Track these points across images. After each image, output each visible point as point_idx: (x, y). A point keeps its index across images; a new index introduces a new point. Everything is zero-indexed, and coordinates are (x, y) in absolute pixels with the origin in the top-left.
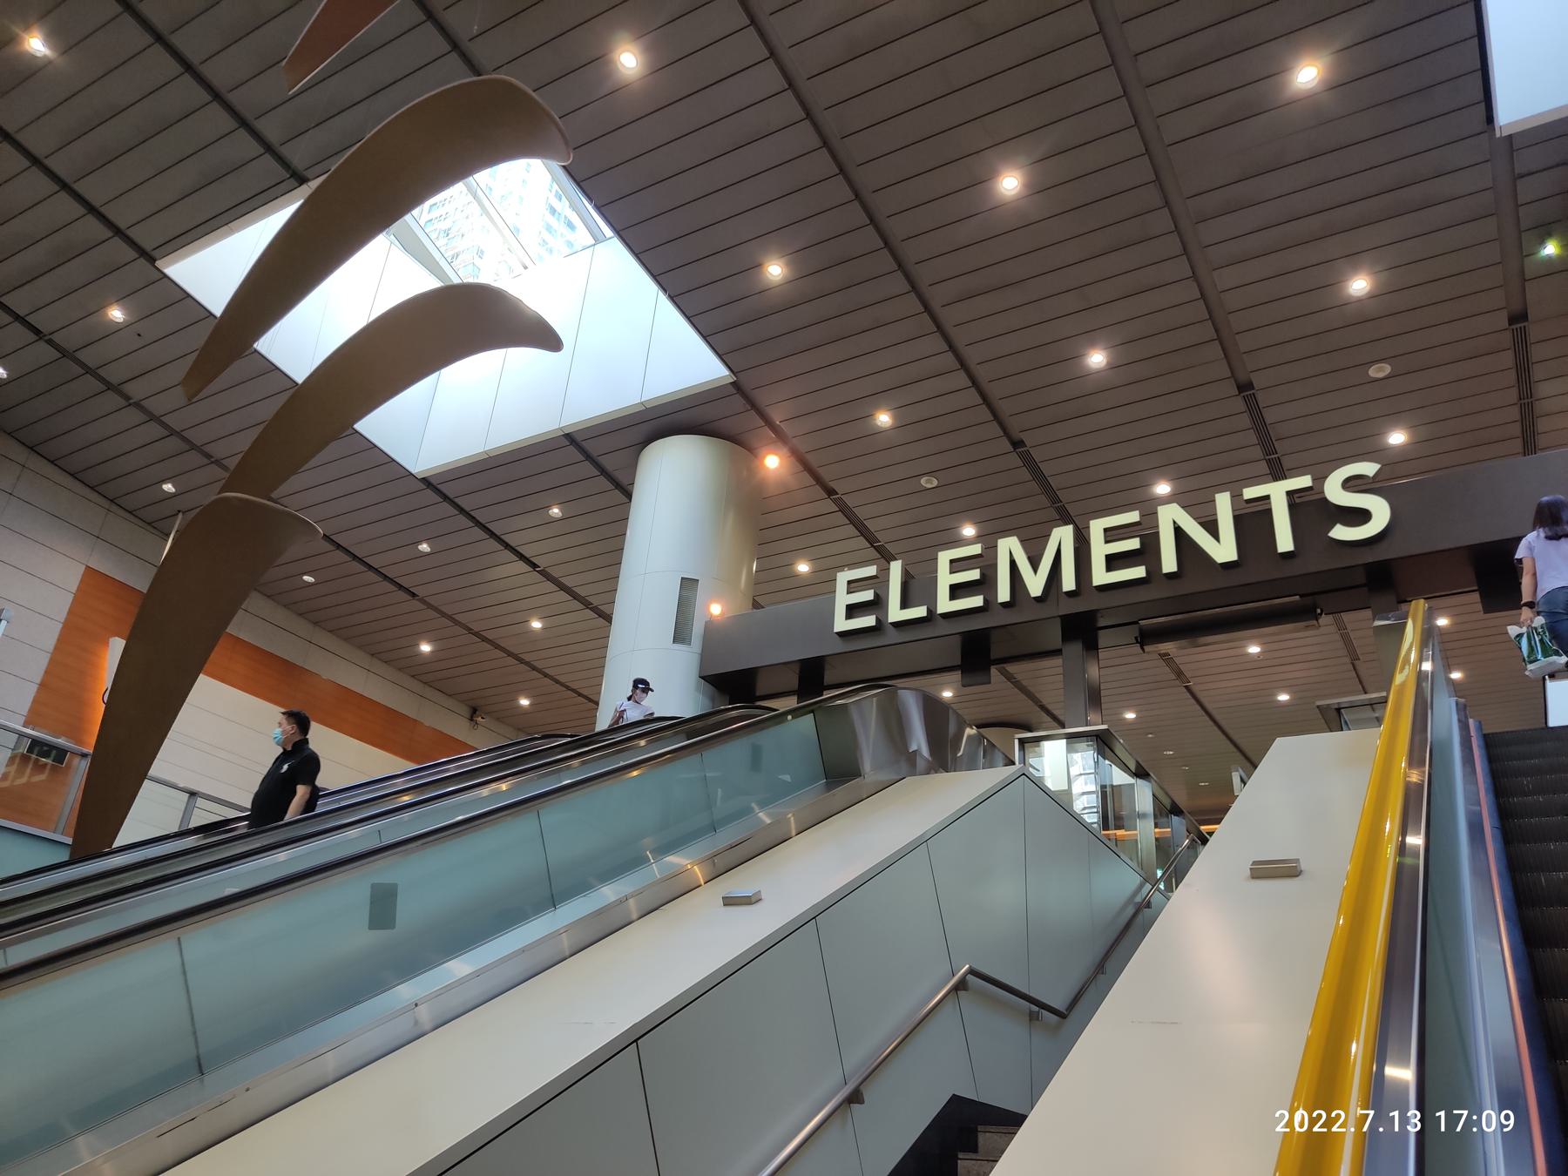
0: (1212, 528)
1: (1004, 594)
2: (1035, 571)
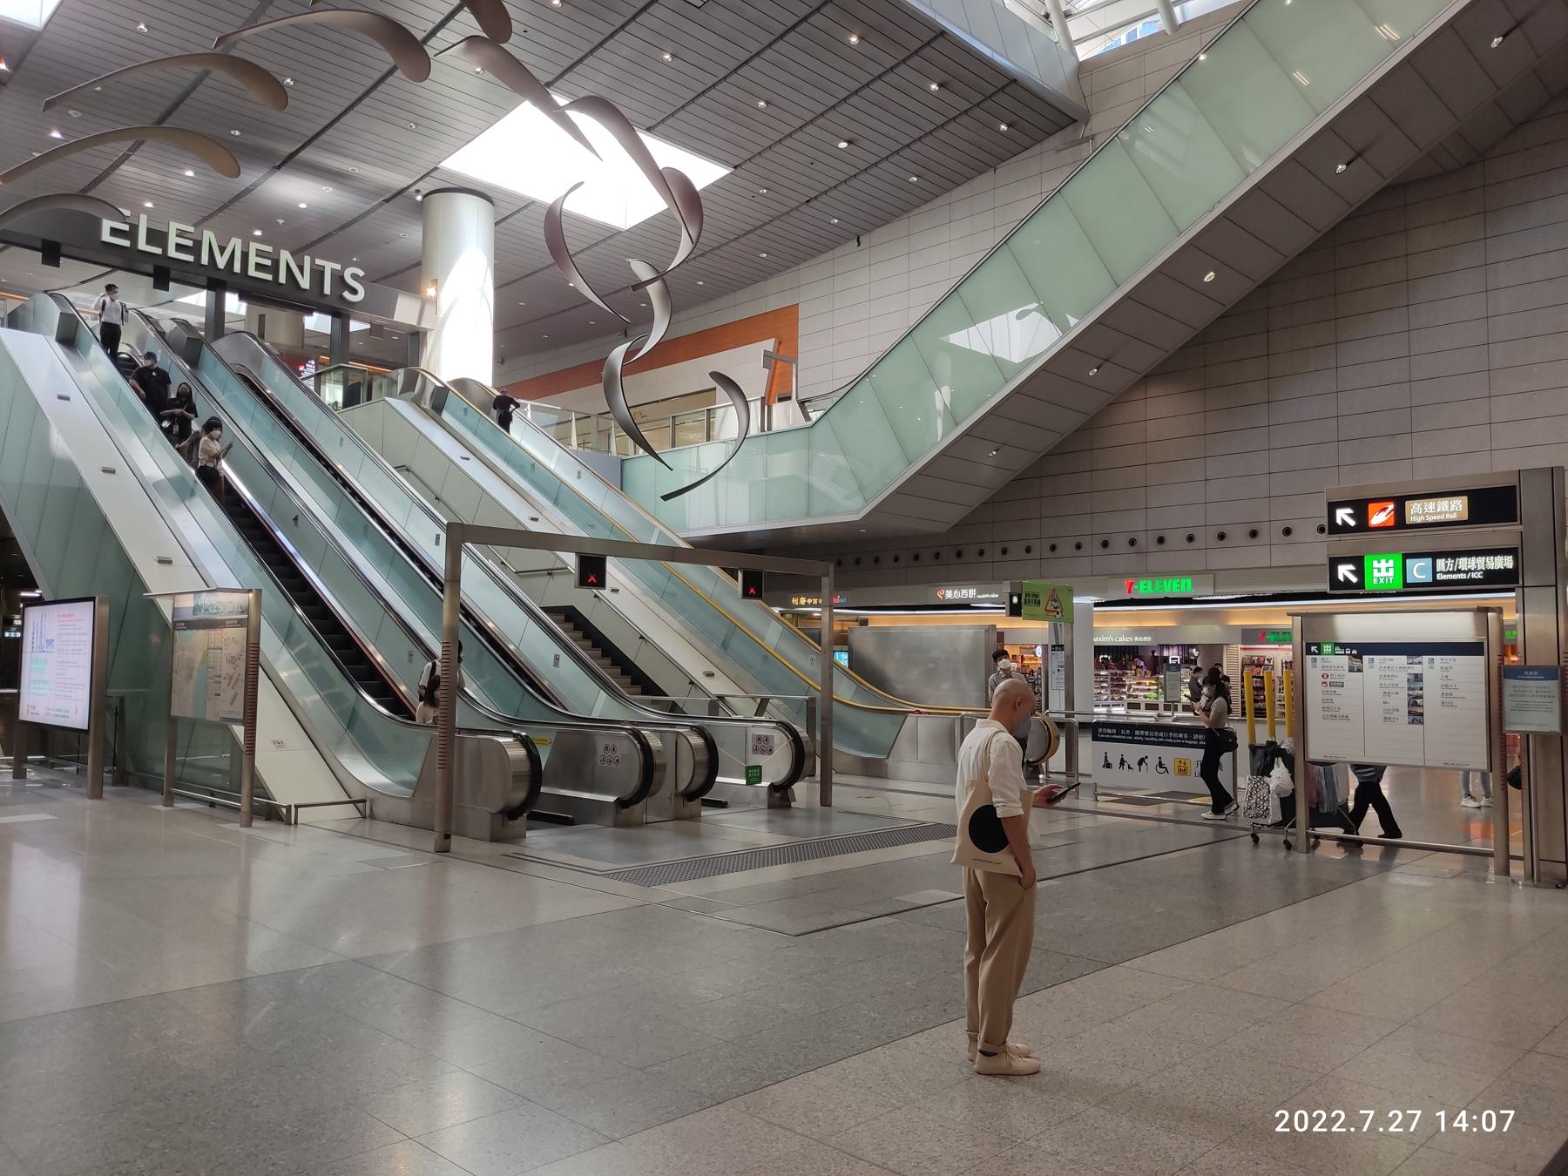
0: (301, 269)
1: (205, 260)
2: (222, 255)
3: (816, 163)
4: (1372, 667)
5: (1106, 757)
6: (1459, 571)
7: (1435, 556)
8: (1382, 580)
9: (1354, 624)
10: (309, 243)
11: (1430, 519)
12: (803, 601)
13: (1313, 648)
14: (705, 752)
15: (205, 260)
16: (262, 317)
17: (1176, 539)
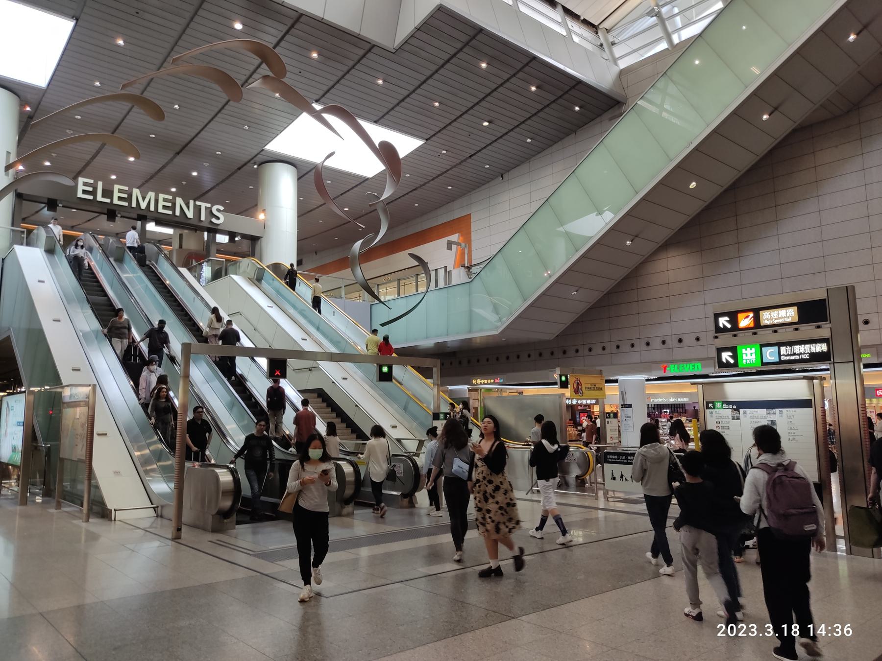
1: (134, 205)
3: (472, 135)
4: (712, 417)
5: (612, 473)
6: (794, 354)
7: (779, 345)
8: (748, 361)
9: (737, 390)
10: (204, 192)
11: (775, 322)
12: (479, 381)
13: (710, 405)
14: (353, 475)
15: (134, 205)
16: (181, 235)
17: (689, 340)
